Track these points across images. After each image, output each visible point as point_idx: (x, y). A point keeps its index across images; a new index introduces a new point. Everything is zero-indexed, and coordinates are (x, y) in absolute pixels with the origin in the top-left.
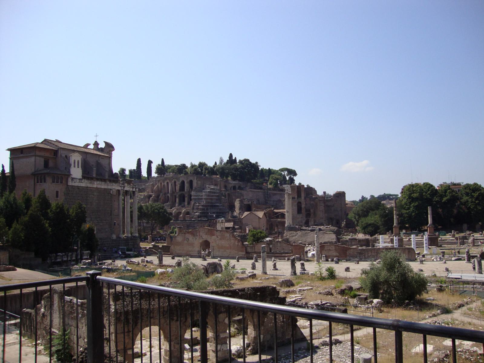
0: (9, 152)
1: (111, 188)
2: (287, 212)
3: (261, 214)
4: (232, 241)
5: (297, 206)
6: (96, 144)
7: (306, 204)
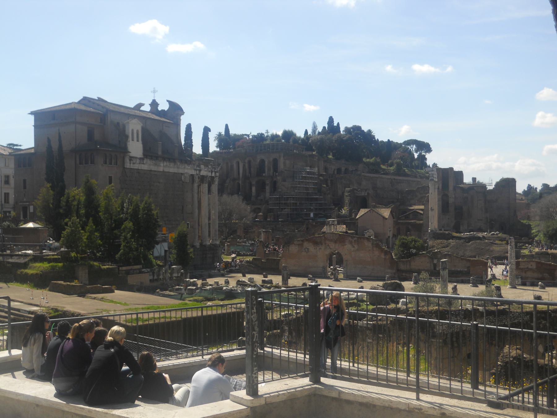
0: (32, 117)
1: (183, 172)
3: (386, 213)
4: (377, 253)
6: (154, 104)
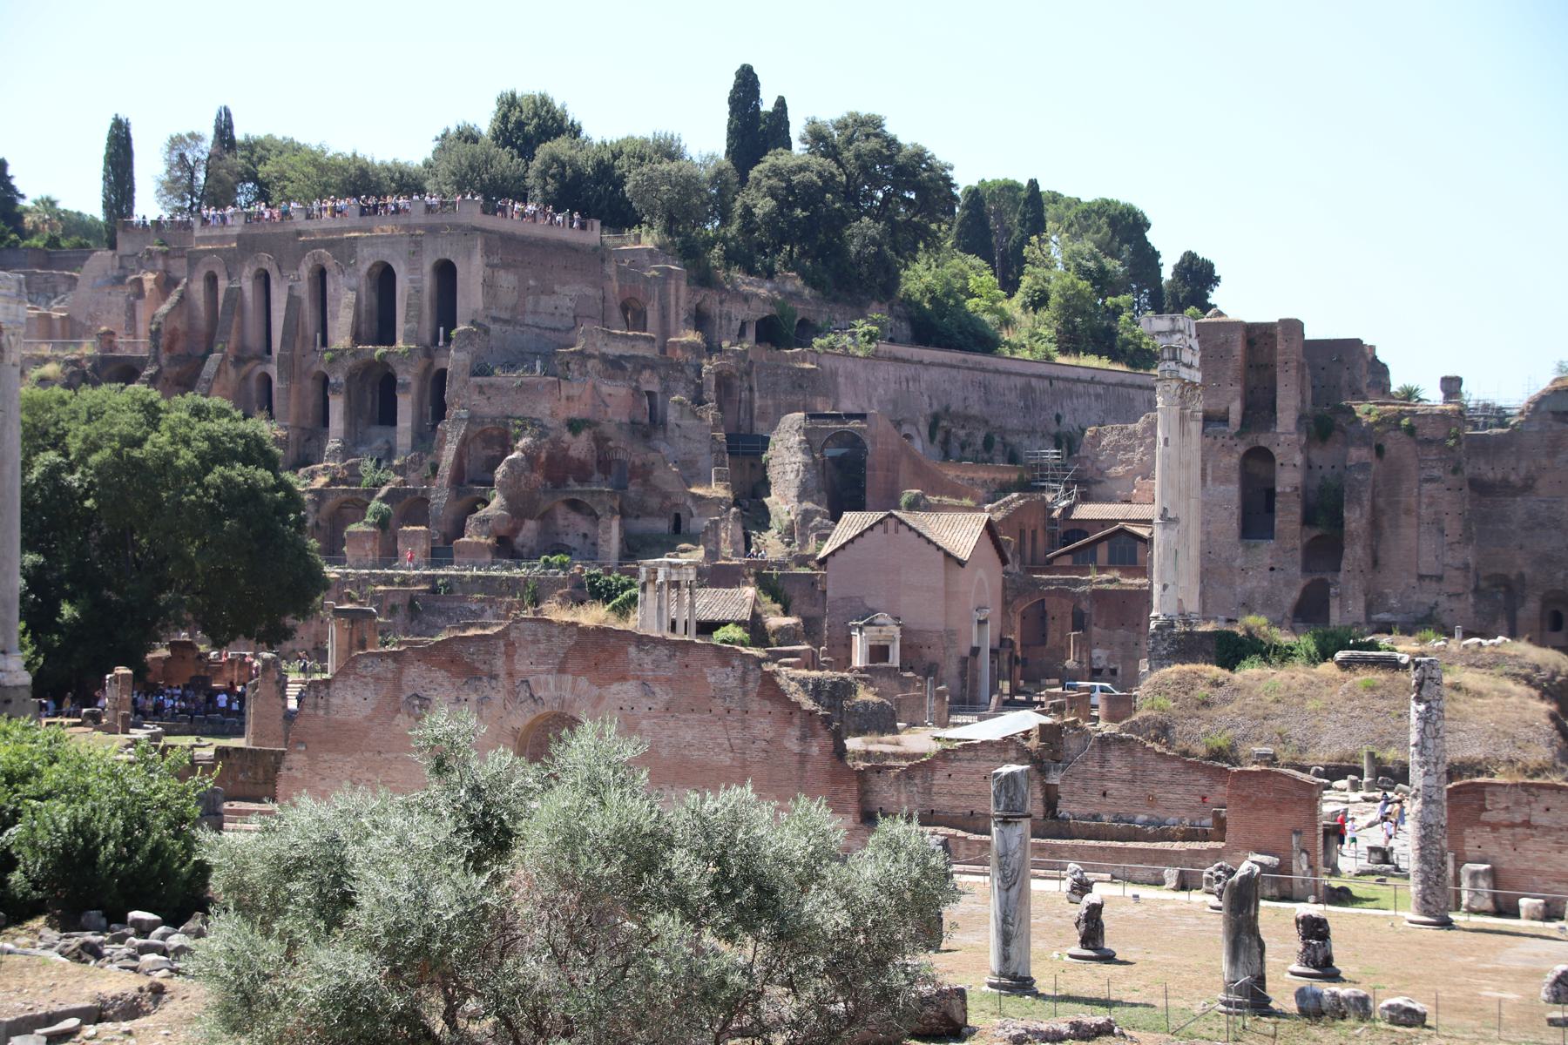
2: (1167, 520)
3: (960, 532)
4: (763, 727)
5: (1235, 476)
7: (1309, 465)
